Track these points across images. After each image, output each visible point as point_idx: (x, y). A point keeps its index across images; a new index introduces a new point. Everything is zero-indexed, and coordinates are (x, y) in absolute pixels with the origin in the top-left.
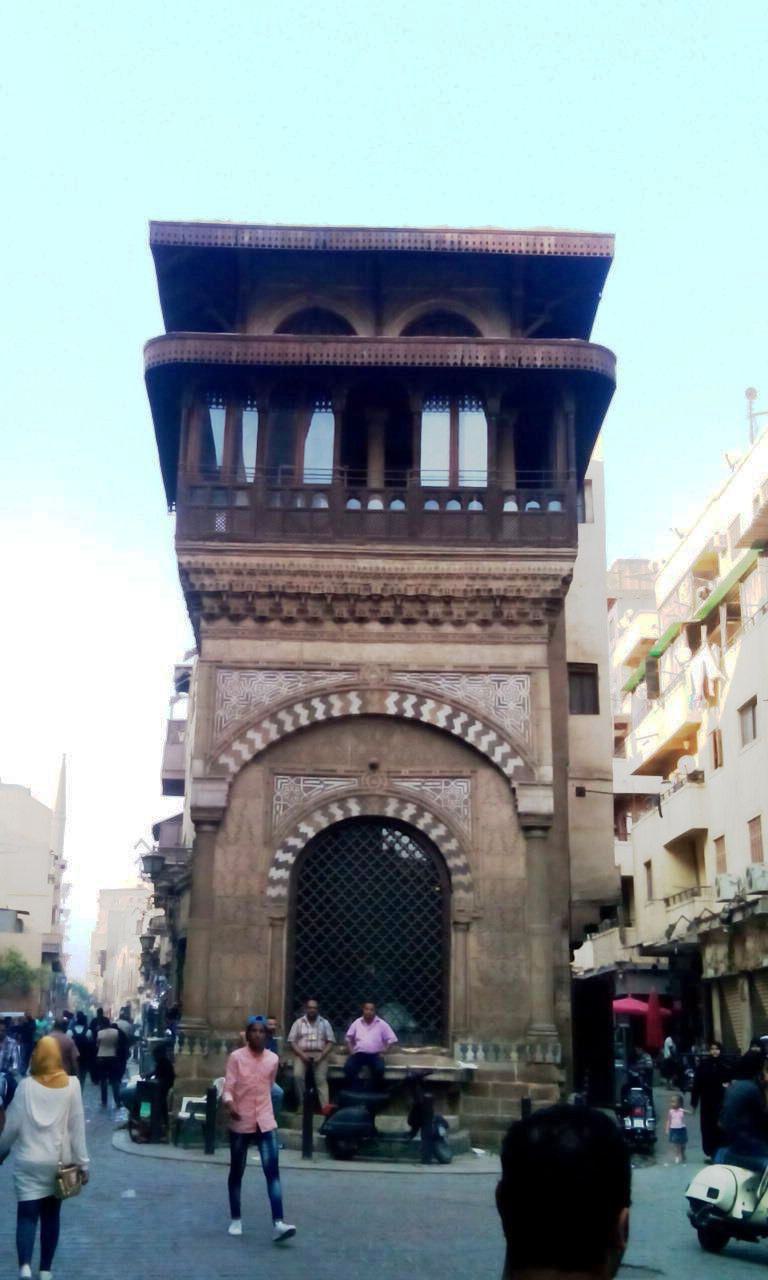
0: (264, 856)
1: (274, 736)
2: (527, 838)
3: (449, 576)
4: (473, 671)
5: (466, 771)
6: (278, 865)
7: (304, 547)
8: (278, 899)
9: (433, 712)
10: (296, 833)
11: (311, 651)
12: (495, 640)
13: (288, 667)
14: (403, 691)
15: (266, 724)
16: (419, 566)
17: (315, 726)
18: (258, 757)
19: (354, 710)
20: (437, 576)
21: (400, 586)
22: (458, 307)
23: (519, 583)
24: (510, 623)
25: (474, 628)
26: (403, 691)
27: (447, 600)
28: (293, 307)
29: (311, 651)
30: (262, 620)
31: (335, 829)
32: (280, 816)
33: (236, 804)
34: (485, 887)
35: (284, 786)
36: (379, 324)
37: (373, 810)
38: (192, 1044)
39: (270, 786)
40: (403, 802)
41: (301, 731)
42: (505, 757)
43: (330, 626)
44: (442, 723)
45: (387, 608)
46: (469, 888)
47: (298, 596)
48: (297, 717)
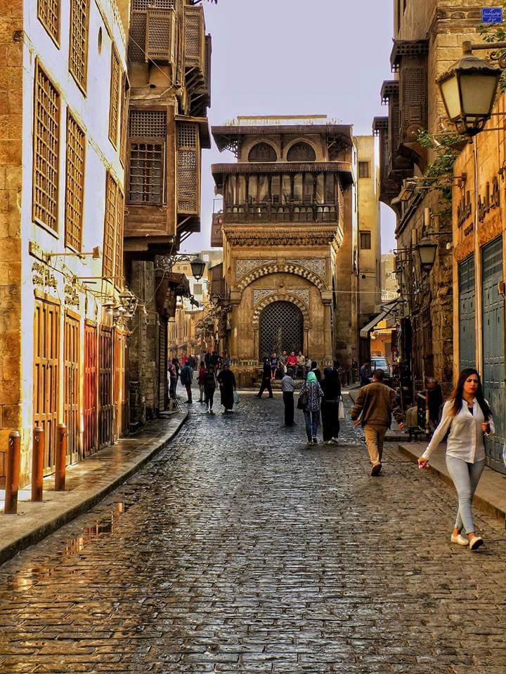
0: (252, 312)
1: (253, 279)
2: (325, 306)
3: (301, 232)
4: (309, 259)
5: (308, 287)
6: (256, 315)
7: (260, 224)
8: (256, 324)
9: (298, 271)
10: (261, 306)
11: (264, 253)
12: (316, 249)
13: (257, 259)
14: (289, 265)
15: (251, 275)
16: (293, 229)
17: (265, 275)
18: (249, 285)
19: (276, 271)
20: (298, 232)
21: (287, 235)
22: (306, 140)
23: (322, 233)
24: (320, 244)
25: (310, 246)
26: (289, 265)
27: (301, 239)
28: (255, 143)
29: (264, 253)
30: (249, 245)
31: (271, 304)
32: (256, 302)
33: (244, 298)
34: (313, 319)
35: (256, 293)
36: (282, 148)
37: (282, 299)
38: (234, 363)
39: (253, 293)
40: (290, 296)
41: (261, 277)
42: (318, 283)
43: (268, 247)
44: (301, 274)
45: (285, 240)
46: (309, 320)
47: (259, 238)
48: (260, 273)
